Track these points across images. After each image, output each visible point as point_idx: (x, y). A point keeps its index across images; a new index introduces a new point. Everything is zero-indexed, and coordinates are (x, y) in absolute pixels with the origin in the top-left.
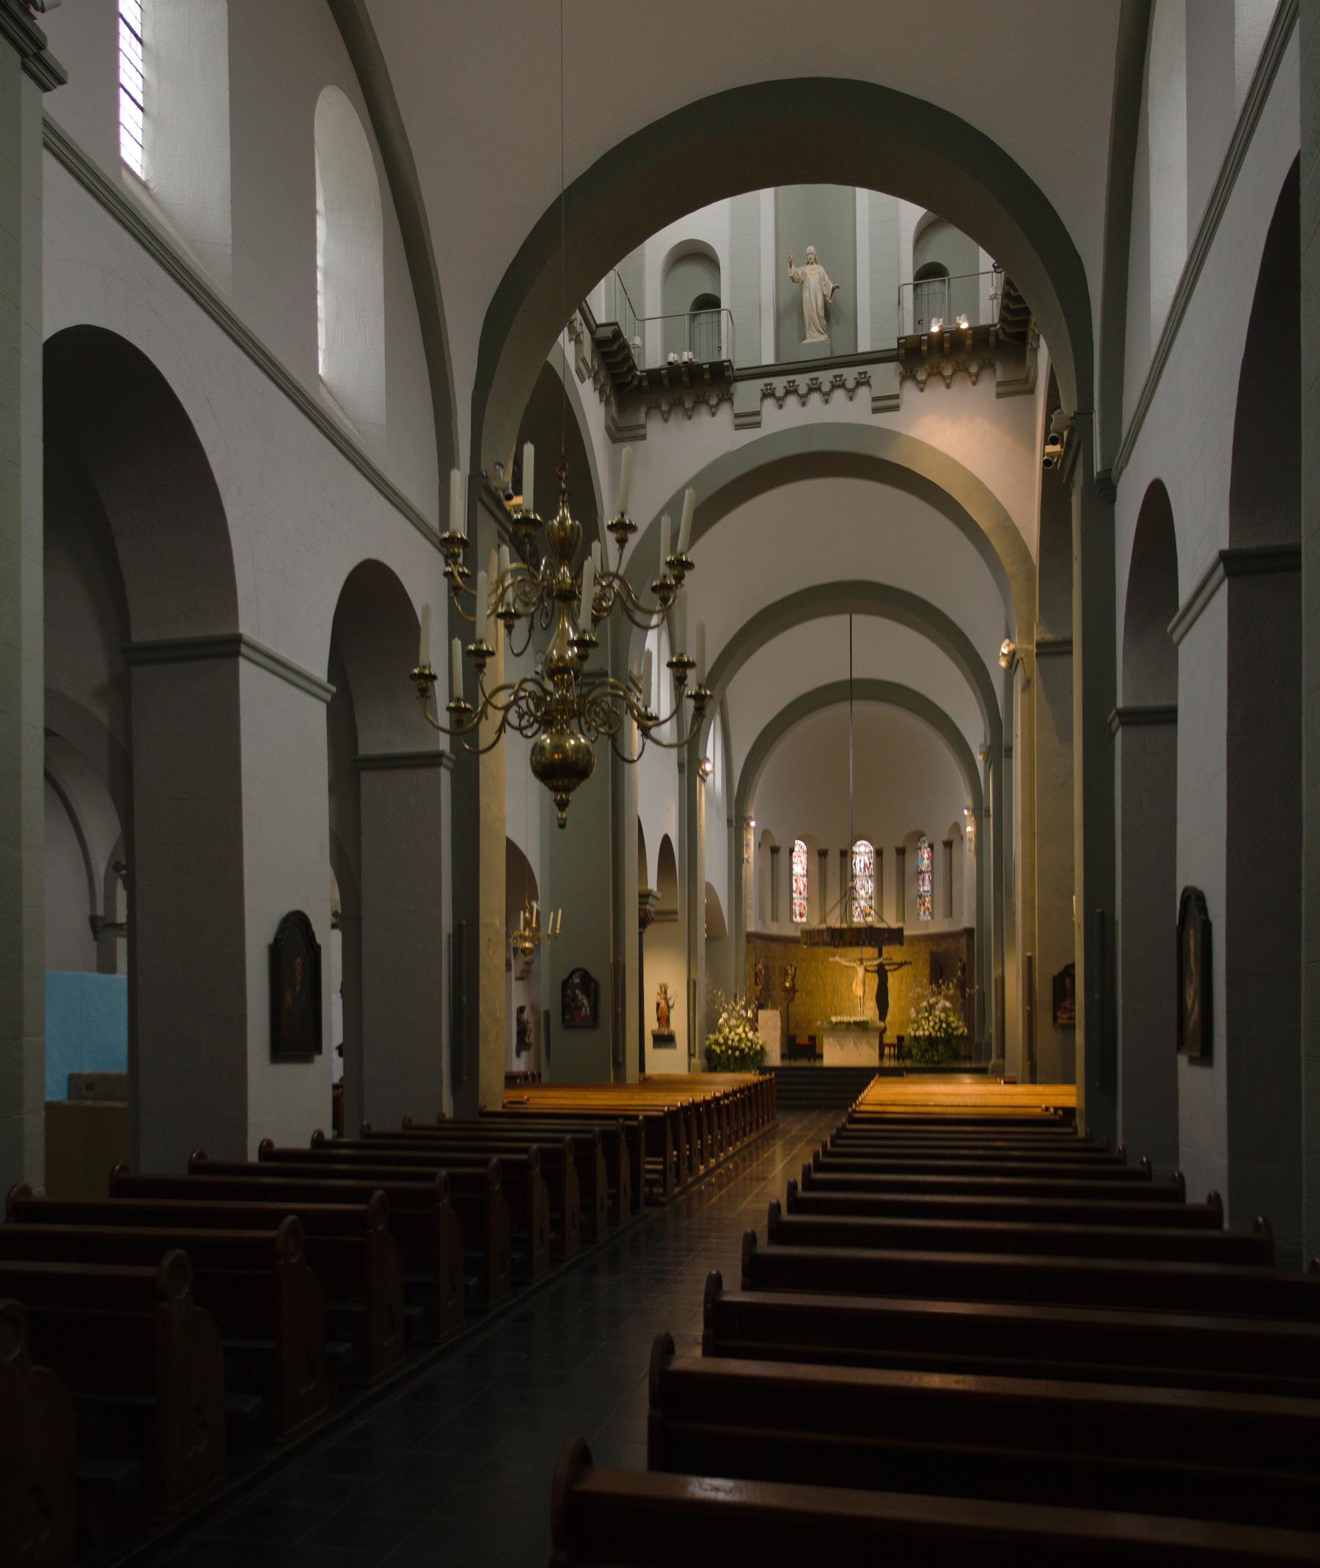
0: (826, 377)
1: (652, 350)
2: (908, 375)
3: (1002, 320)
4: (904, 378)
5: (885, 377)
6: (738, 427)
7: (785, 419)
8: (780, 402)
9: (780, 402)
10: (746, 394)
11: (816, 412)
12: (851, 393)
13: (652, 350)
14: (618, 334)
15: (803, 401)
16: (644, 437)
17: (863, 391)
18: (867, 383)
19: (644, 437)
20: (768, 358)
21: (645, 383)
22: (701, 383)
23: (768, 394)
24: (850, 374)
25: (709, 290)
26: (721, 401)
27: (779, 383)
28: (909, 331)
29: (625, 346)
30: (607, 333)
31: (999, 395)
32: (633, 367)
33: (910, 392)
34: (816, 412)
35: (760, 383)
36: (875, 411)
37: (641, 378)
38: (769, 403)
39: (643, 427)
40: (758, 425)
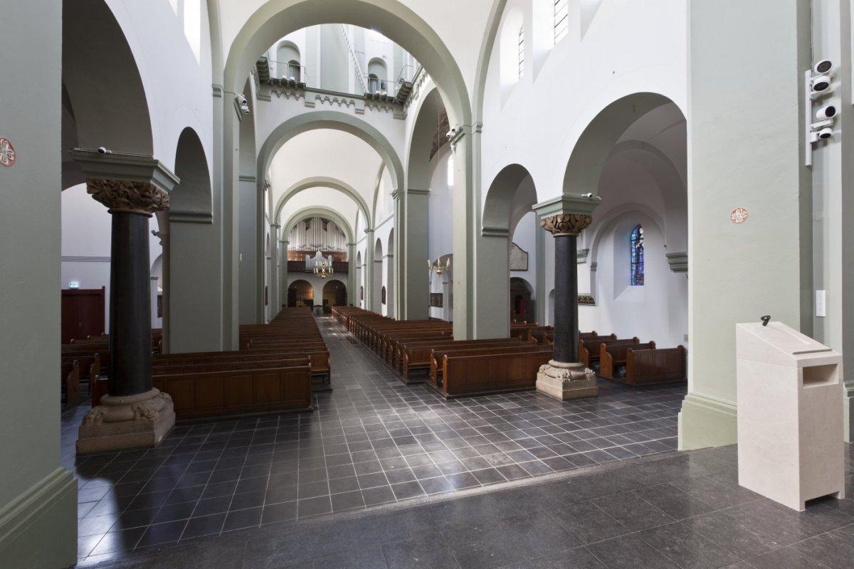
0: (340, 99)
1: (274, 74)
2: (367, 105)
3: (398, 96)
4: (365, 105)
5: (360, 104)
6: (306, 106)
7: (322, 107)
8: (322, 102)
9: (322, 102)
10: (310, 96)
11: (335, 108)
12: (348, 106)
13: (274, 74)
14: (266, 62)
15: (331, 103)
16: (270, 101)
17: (352, 106)
18: (354, 104)
19: (270, 101)
20: (318, 87)
21: (272, 82)
22: (294, 88)
23: (318, 98)
24: (348, 100)
25: (295, 59)
26: (301, 96)
27: (323, 96)
28: (368, 92)
29: (267, 67)
30: (263, 60)
31: (394, 118)
32: (268, 76)
33: (367, 109)
34: (335, 108)
35: (316, 94)
36: (356, 113)
37: (270, 81)
38: (318, 102)
39: (270, 97)
40: (313, 107)
